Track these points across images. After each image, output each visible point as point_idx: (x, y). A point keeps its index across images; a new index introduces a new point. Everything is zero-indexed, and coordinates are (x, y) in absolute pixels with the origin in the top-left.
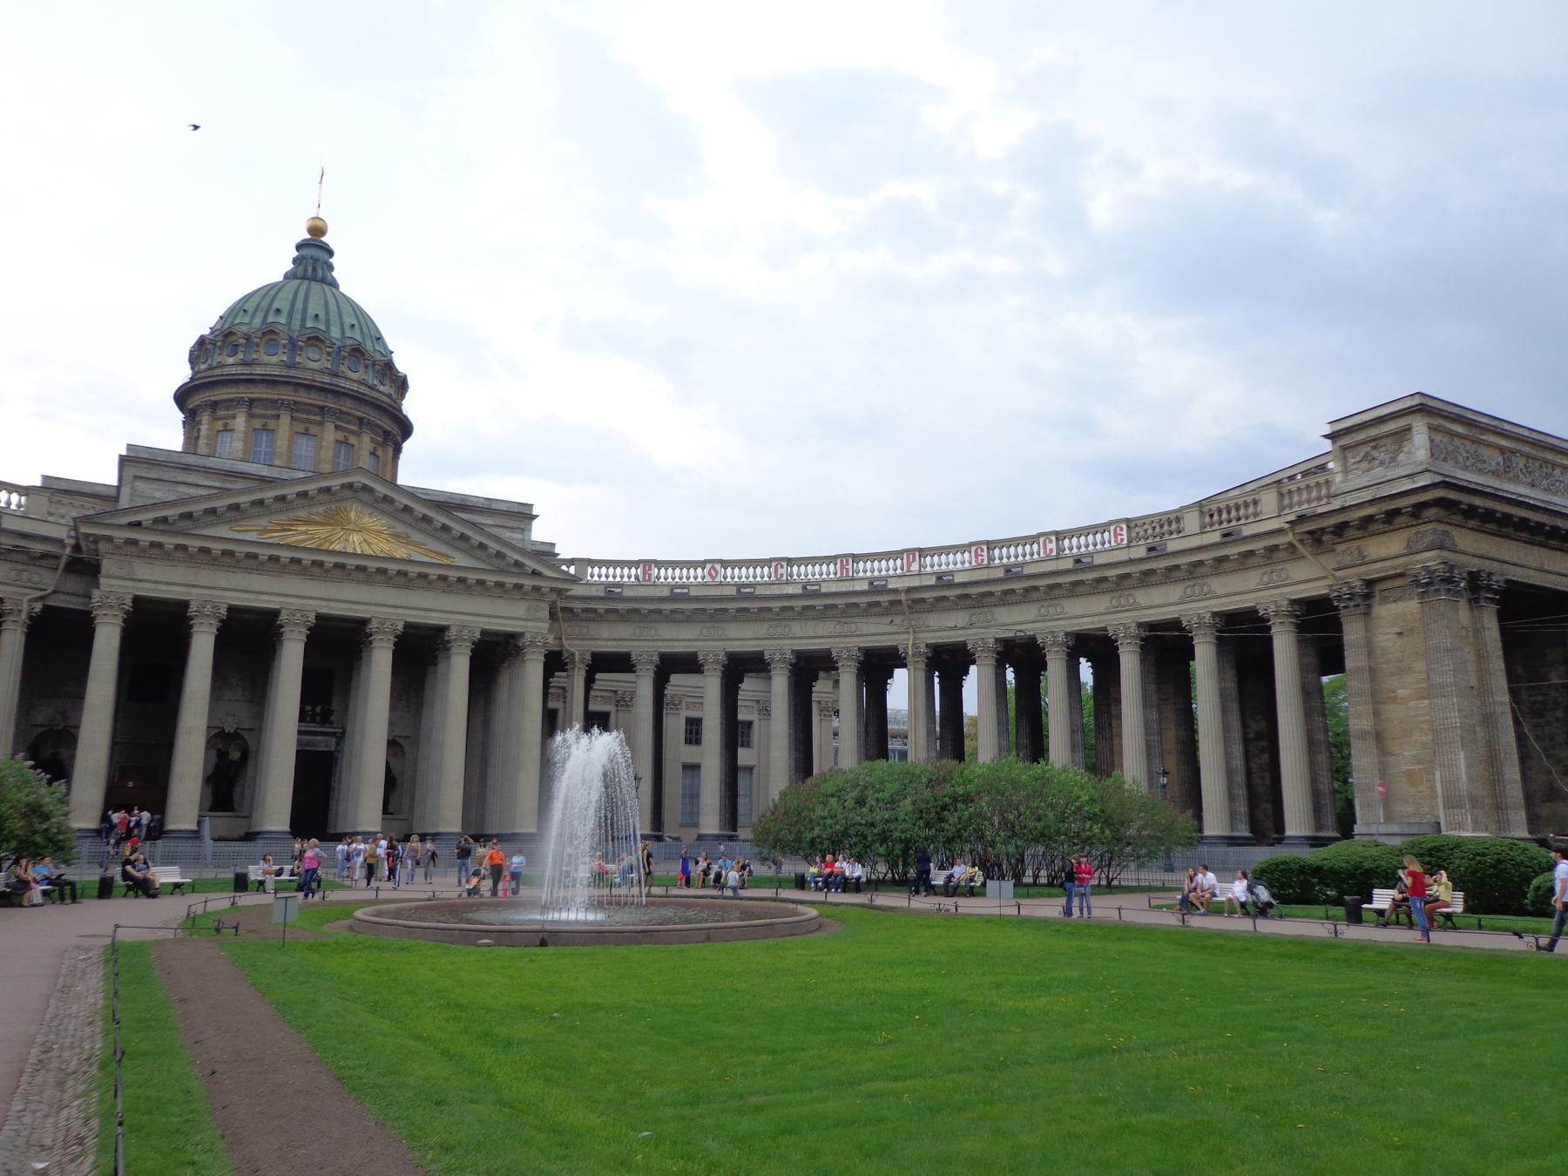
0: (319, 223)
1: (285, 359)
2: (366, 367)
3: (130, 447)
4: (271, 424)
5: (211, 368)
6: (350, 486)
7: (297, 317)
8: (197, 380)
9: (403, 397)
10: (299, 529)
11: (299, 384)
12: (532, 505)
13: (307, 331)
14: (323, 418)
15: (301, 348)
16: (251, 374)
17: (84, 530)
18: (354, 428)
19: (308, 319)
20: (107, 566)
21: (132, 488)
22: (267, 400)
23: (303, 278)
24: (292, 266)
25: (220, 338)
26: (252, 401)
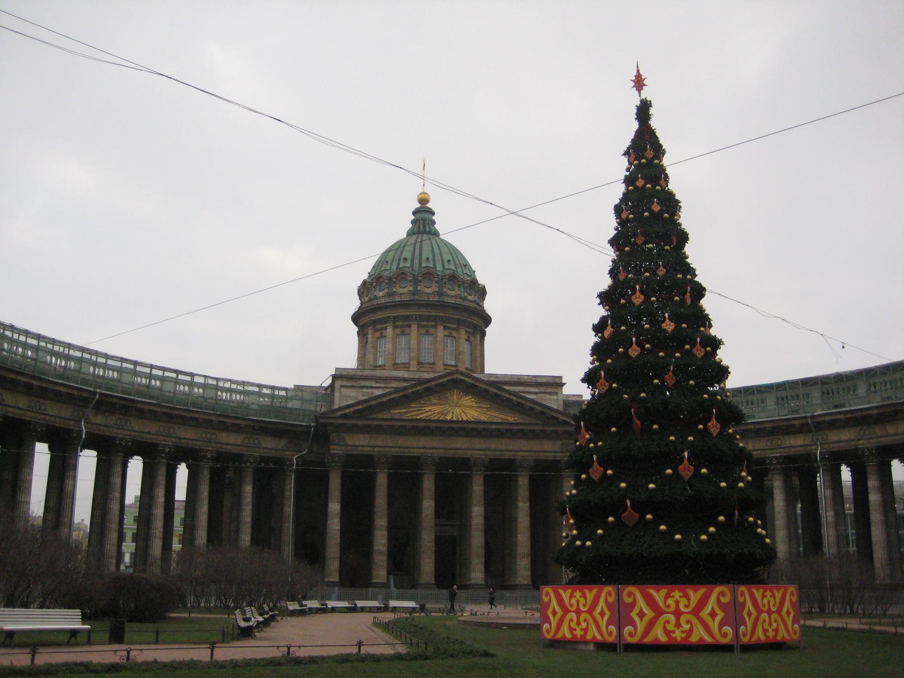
0: (423, 196)
1: (412, 289)
2: (459, 286)
3: (337, 369)
4: (406, 330)
5: (371, 300)
6: (453, 381)
7: (416, 261)
9: (484, 299)
12: (561, 377)
13: (423, 270)
14: (436, 323)
15: (420, 281)
16: (393, 302)
17: (321, 421)
18: (455, 326)
19: (423, 262)
20: (334, 437)
21: (340, 392)
22: (403, 316)
23: (419, 233)
24: (411, 225)
25: (374, 281)
26: (394, 318)
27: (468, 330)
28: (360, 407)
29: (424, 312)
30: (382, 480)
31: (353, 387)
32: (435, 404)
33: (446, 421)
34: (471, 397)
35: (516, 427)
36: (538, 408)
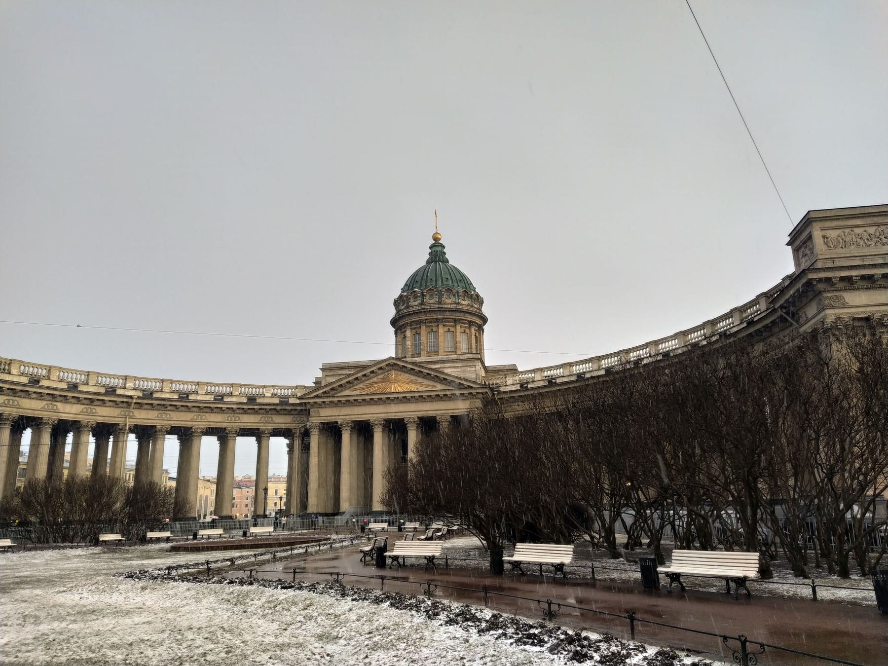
2: (454, 295)
3: (323, 364)
7: (424, 281)
20: (313, 412)
26: (411, 322)
29: (429, 317)
30: (346, 437)
32: (380, 382)
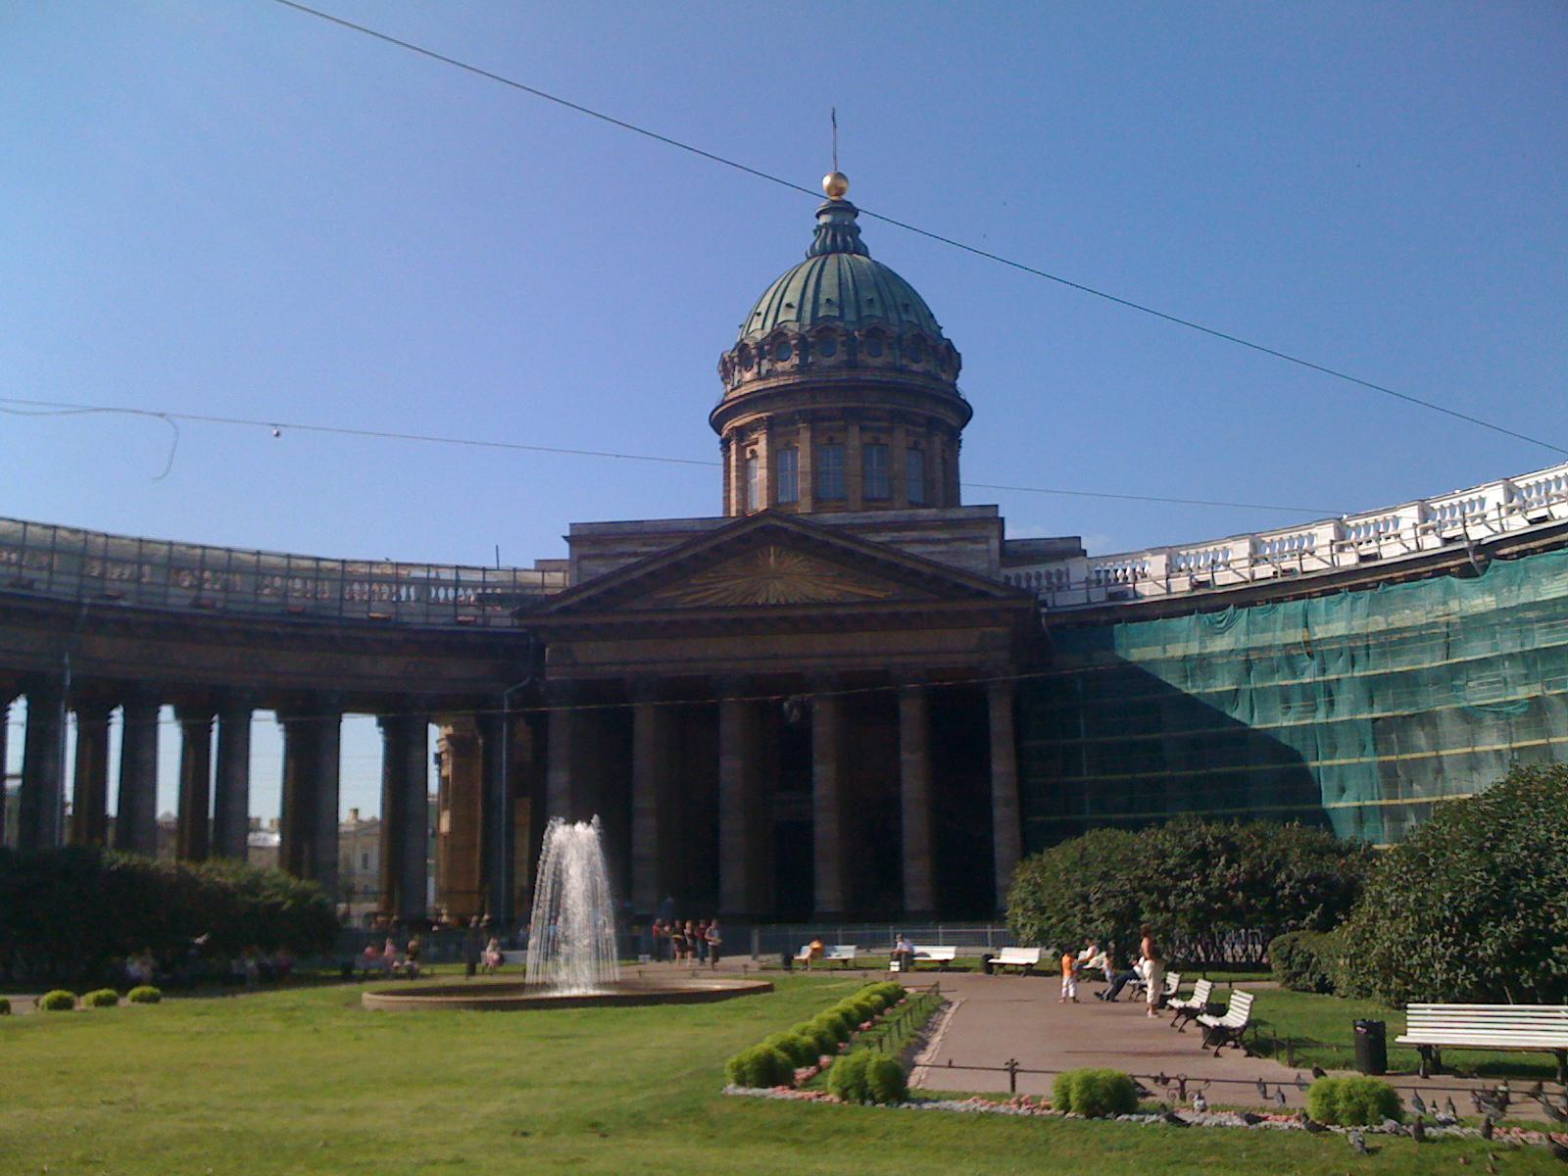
2: (890, 347)
6: (763, 529)
7: (808, 307)
8: (727, 402)
10: (719, 586)
11: (812, 389)
12: (997, 506)
18: (884, 424)
21: (579, 569)
27: (911, 428)
28: (592, 592)
30: (645, 724)
31: (601, 556)
33: (756, 606)
34: (801, 558)
35: (885, 610)
36: (927, 570)
